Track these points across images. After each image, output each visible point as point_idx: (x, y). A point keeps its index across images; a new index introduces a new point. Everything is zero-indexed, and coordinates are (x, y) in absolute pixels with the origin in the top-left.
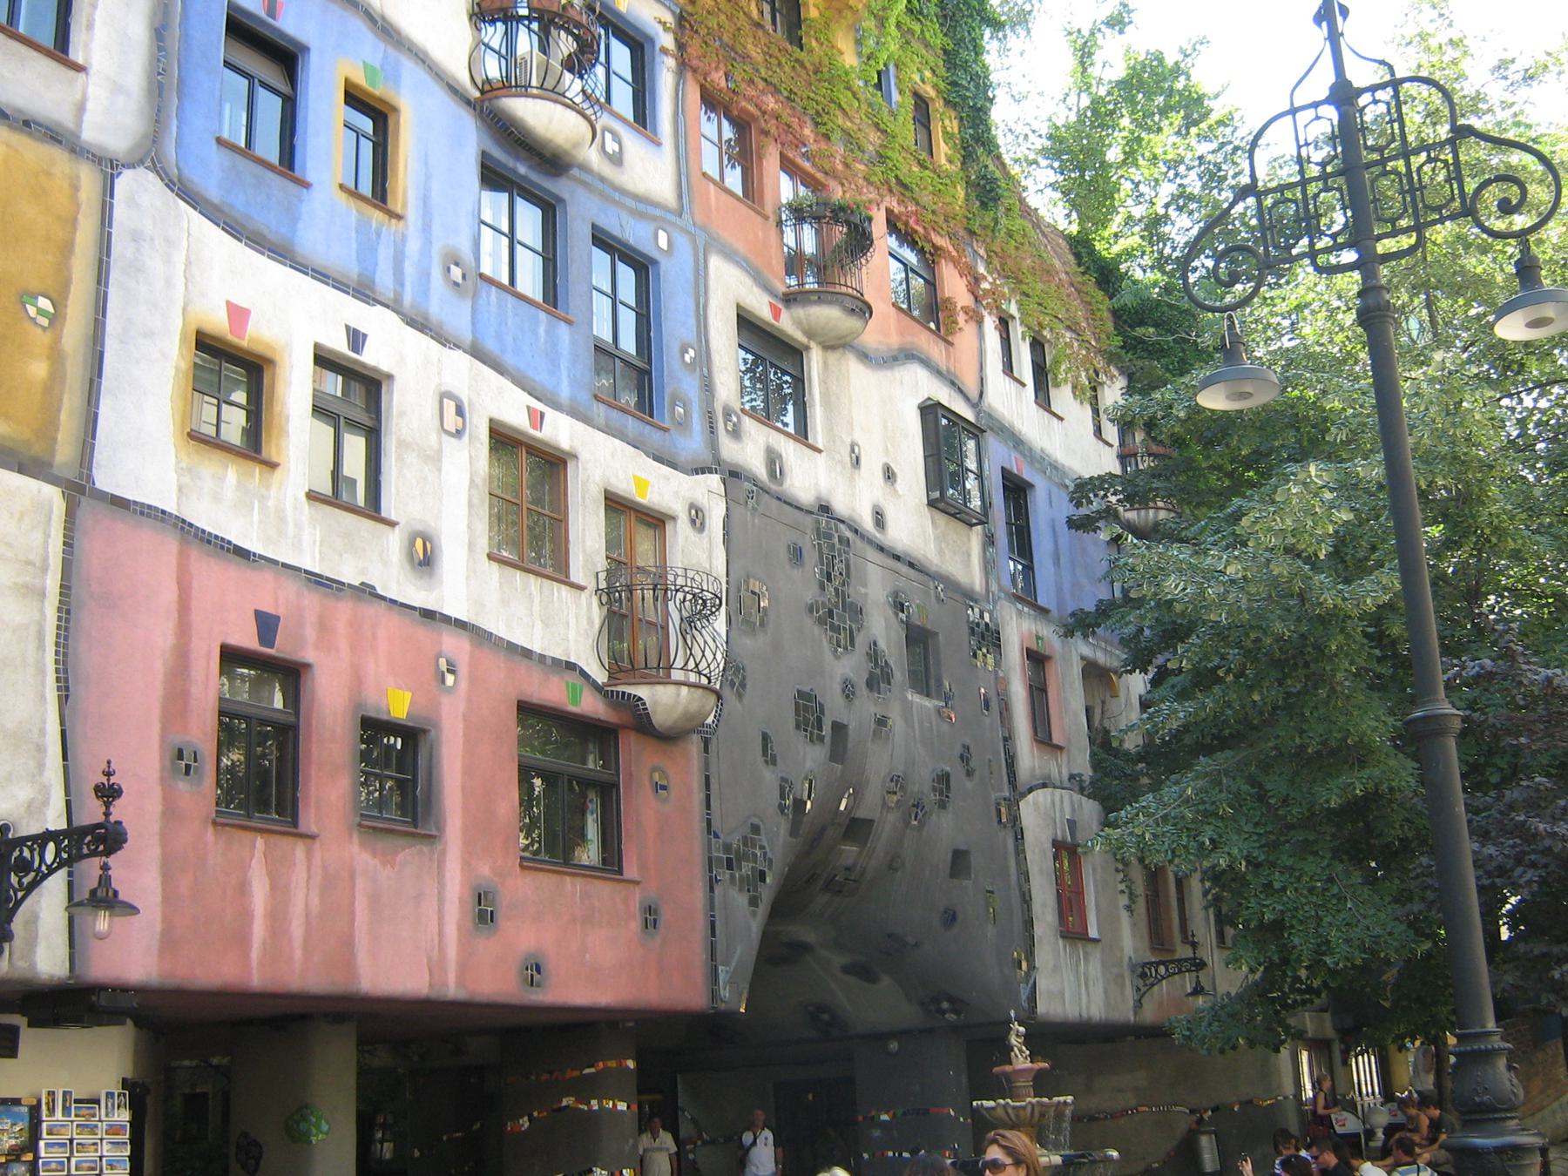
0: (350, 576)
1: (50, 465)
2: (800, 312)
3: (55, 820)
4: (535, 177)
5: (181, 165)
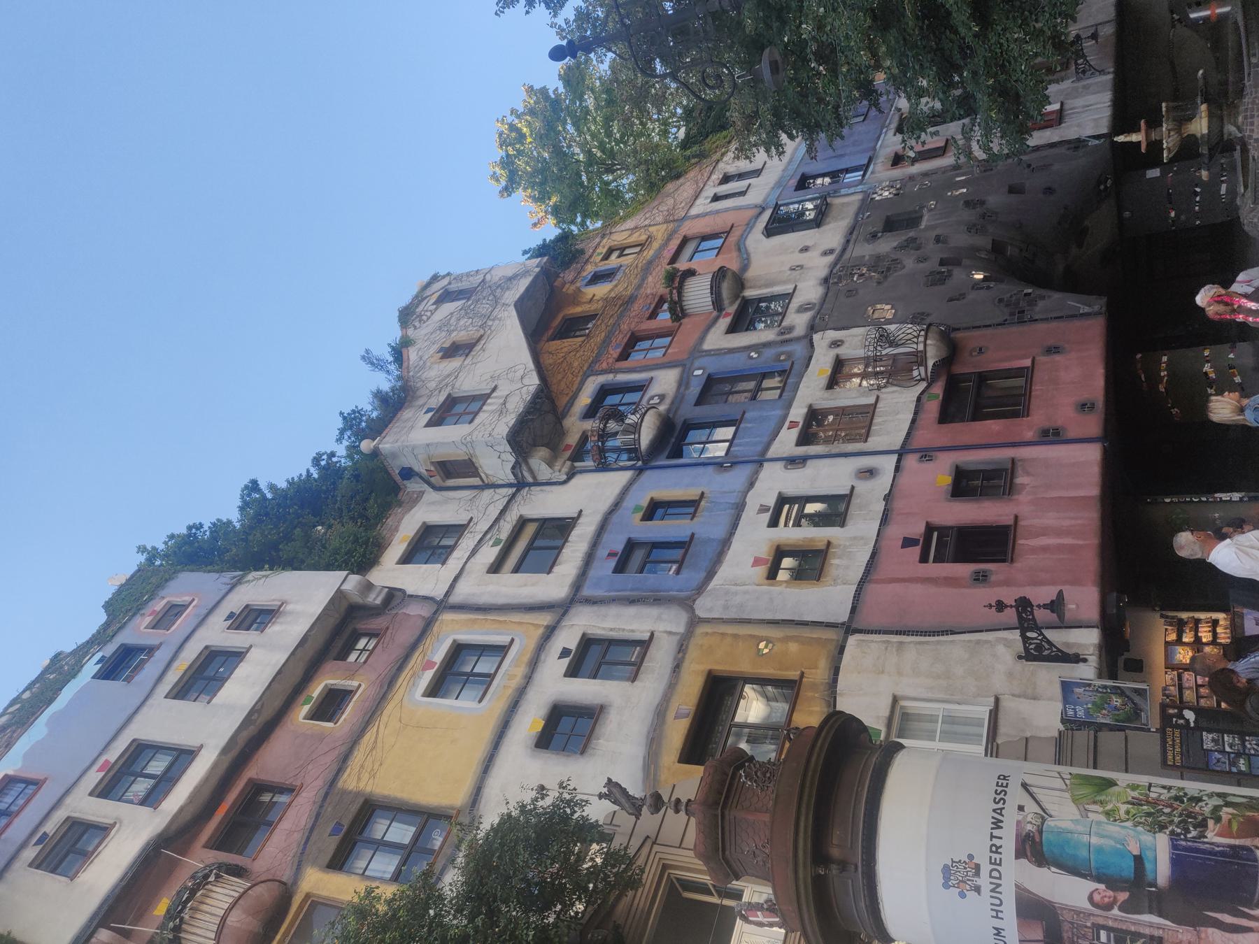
0: (880, 506)
2: (726, 302)
3: (1015, 635)
4: (676, 434)
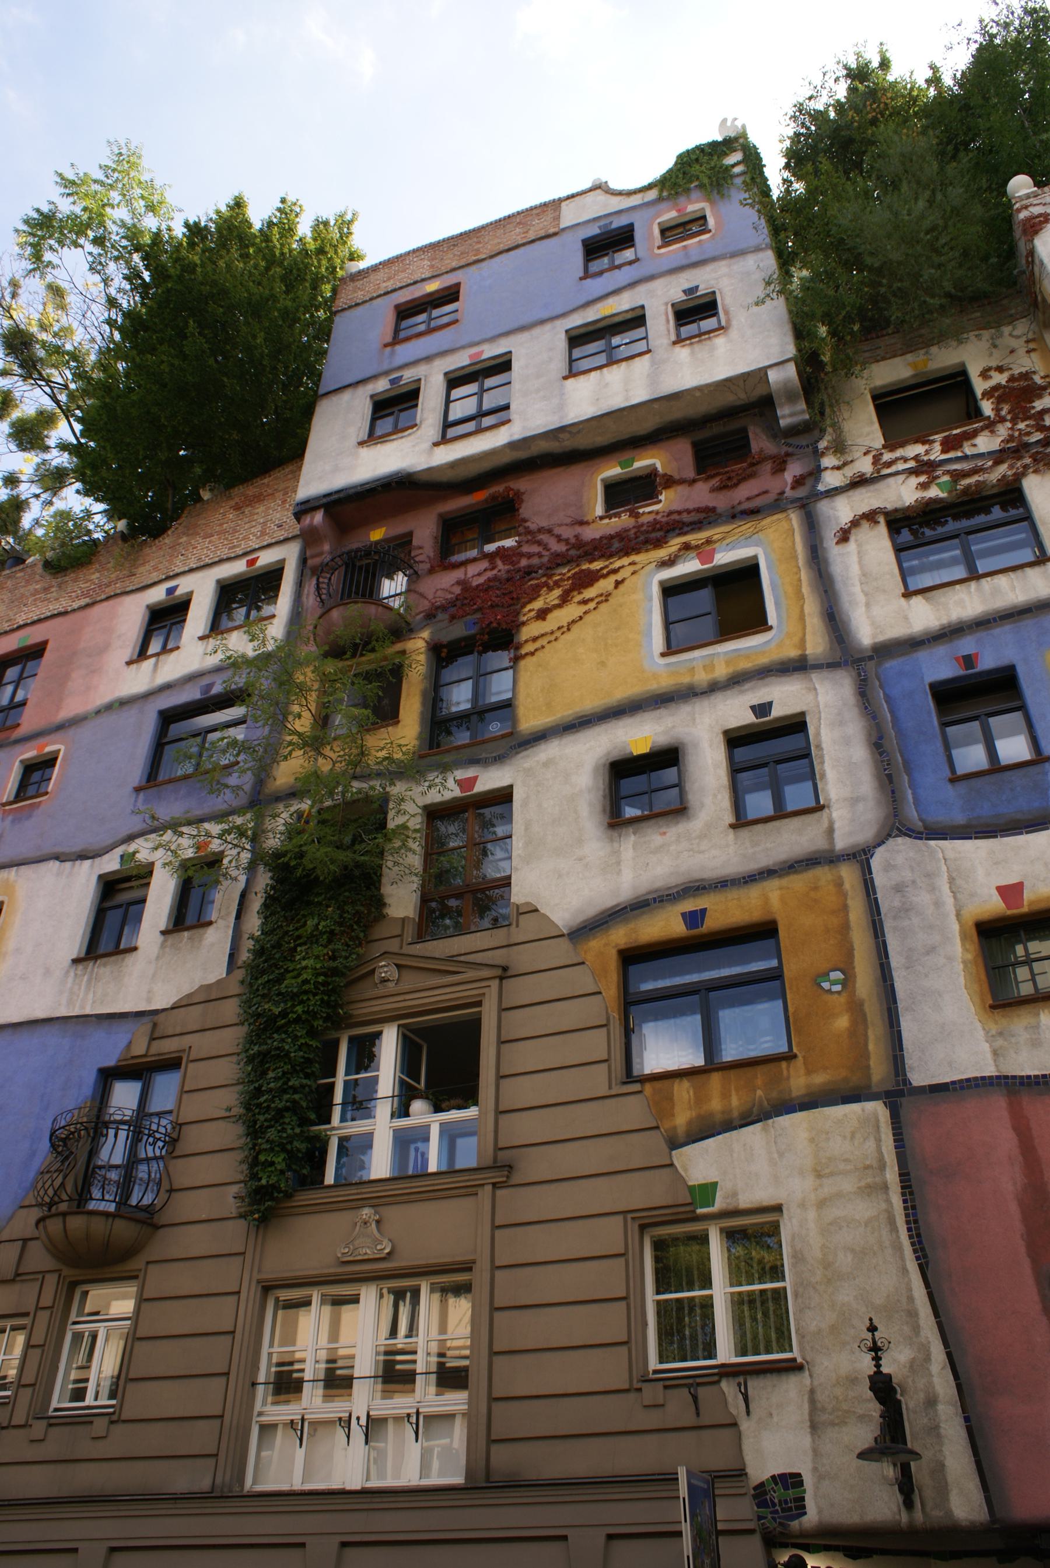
1: (869, 1087)
5: (924, 817)
